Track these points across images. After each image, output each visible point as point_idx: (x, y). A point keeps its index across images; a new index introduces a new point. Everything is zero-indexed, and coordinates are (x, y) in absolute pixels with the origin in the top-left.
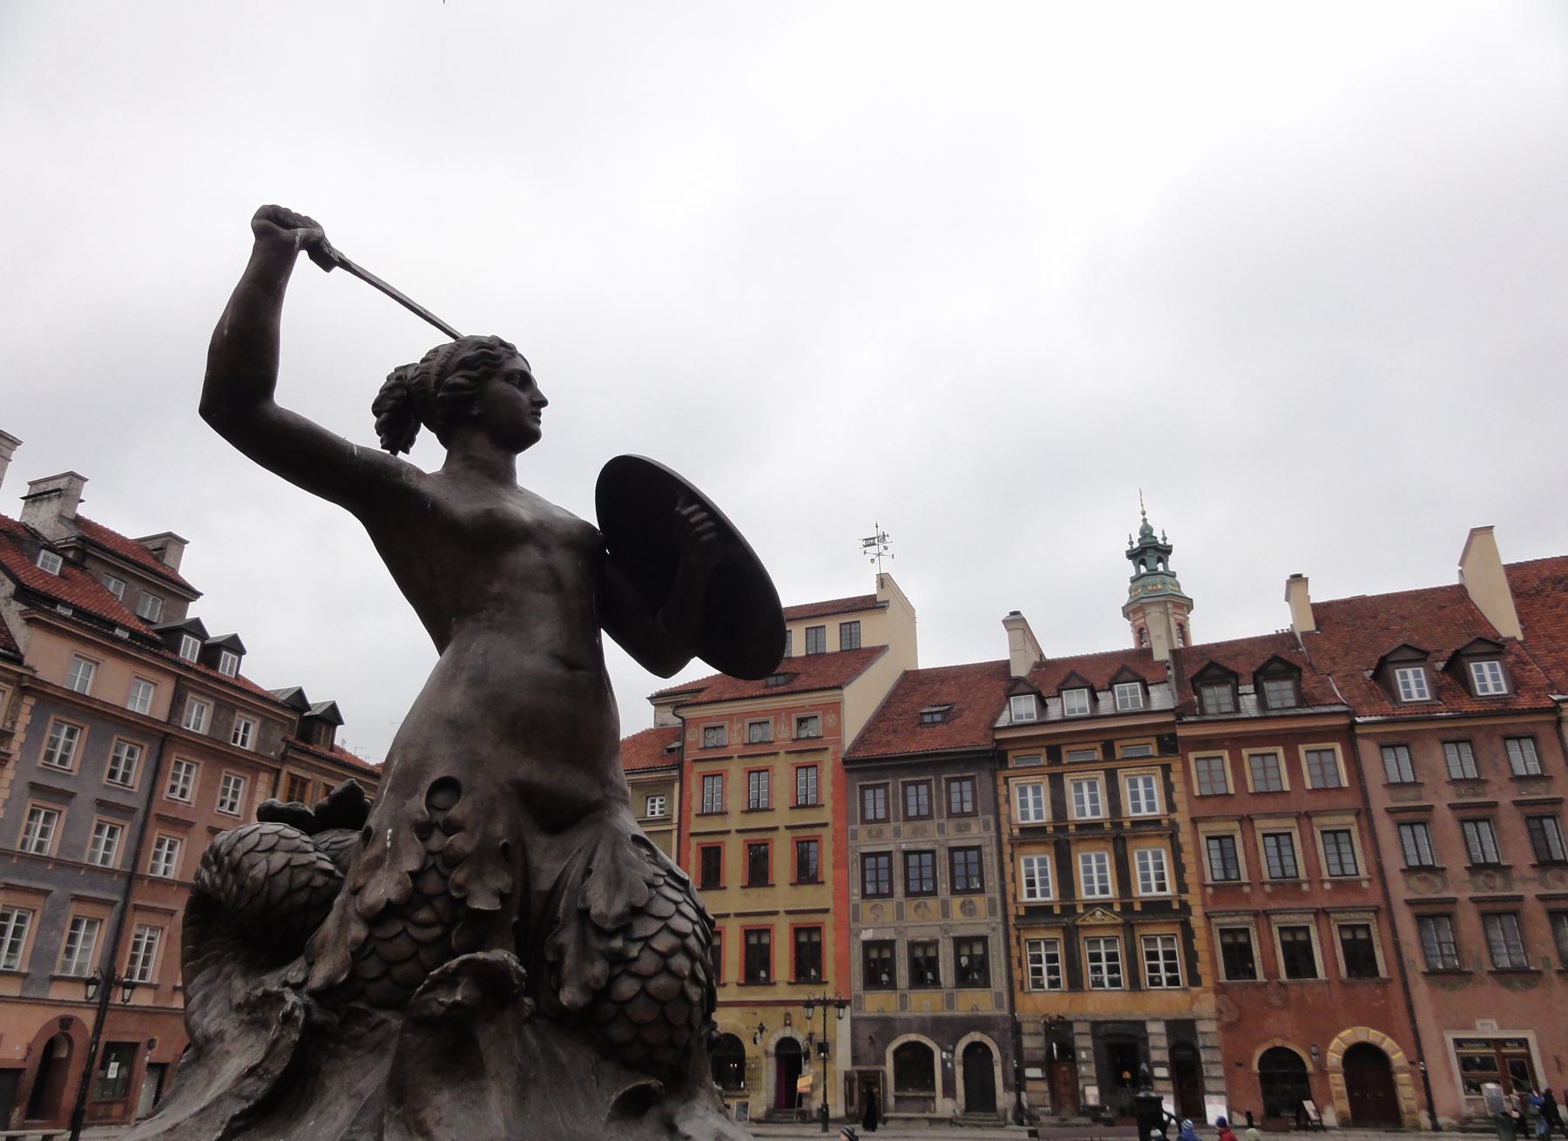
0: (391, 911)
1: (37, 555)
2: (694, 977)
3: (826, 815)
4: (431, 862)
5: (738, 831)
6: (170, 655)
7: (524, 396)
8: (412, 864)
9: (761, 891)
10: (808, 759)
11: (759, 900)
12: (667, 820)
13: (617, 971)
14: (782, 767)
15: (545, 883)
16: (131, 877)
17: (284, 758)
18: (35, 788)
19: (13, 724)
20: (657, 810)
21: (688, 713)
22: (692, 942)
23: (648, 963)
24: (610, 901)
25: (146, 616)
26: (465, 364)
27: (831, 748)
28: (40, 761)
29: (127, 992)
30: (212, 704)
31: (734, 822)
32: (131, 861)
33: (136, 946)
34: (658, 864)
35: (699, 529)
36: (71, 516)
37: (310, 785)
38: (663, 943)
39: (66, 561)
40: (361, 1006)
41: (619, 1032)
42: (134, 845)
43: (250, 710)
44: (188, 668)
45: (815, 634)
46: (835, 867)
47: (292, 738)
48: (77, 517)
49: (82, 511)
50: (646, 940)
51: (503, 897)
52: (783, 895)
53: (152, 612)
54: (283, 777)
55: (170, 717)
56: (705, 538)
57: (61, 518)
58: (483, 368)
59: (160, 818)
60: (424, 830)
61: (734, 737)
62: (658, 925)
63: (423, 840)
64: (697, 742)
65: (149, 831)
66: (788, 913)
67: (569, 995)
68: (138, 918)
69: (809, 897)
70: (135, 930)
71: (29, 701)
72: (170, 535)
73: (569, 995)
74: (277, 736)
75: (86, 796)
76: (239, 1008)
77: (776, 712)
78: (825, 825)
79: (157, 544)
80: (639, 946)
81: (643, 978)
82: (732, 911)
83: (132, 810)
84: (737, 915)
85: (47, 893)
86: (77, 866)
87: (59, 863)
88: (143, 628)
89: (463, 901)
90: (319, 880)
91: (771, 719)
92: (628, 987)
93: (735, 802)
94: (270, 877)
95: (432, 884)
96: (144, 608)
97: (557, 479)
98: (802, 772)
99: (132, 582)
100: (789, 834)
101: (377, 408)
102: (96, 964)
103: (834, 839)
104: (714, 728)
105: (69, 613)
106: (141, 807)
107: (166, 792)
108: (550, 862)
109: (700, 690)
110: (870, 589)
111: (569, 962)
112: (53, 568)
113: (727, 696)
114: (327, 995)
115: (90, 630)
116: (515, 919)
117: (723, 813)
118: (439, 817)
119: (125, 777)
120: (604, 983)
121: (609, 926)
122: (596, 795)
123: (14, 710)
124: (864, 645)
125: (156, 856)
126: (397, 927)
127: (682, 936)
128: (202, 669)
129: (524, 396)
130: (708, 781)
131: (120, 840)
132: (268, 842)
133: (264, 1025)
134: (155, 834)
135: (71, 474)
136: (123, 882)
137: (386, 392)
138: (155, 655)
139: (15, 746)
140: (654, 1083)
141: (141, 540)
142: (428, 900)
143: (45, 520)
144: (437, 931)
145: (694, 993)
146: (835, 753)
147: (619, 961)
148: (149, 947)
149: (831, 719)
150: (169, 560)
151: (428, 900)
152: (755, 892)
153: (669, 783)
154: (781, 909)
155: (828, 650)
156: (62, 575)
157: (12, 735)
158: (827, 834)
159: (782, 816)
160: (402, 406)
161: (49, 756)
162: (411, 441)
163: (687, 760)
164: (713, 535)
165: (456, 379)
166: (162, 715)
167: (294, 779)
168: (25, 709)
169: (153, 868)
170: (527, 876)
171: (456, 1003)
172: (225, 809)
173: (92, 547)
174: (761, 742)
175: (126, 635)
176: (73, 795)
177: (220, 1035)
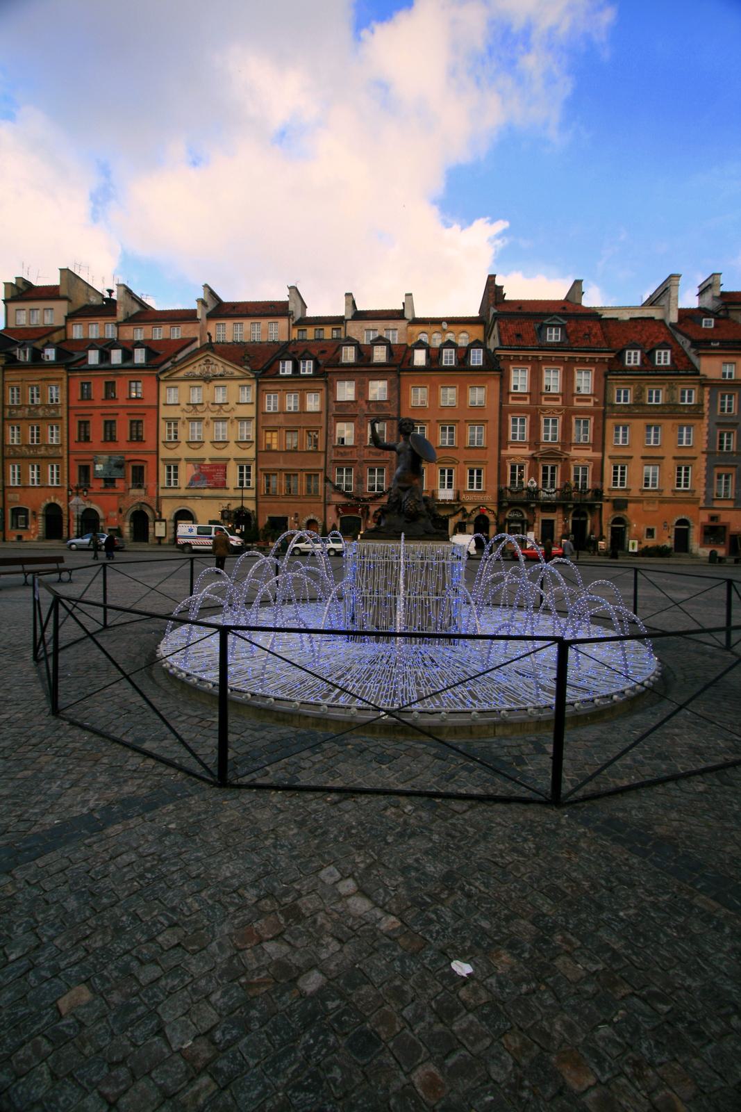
18: (718, 424)
19: (702, 400)
28: (719, 413)
36: (718, 294)
39: (718, 319)
49: (722, 289)
57: (714, 298)
71: (707, 389)
135: (713, 275)
139: (705, 409)
143: (708, 302)
156: (716, 326)
157: (702, 405)
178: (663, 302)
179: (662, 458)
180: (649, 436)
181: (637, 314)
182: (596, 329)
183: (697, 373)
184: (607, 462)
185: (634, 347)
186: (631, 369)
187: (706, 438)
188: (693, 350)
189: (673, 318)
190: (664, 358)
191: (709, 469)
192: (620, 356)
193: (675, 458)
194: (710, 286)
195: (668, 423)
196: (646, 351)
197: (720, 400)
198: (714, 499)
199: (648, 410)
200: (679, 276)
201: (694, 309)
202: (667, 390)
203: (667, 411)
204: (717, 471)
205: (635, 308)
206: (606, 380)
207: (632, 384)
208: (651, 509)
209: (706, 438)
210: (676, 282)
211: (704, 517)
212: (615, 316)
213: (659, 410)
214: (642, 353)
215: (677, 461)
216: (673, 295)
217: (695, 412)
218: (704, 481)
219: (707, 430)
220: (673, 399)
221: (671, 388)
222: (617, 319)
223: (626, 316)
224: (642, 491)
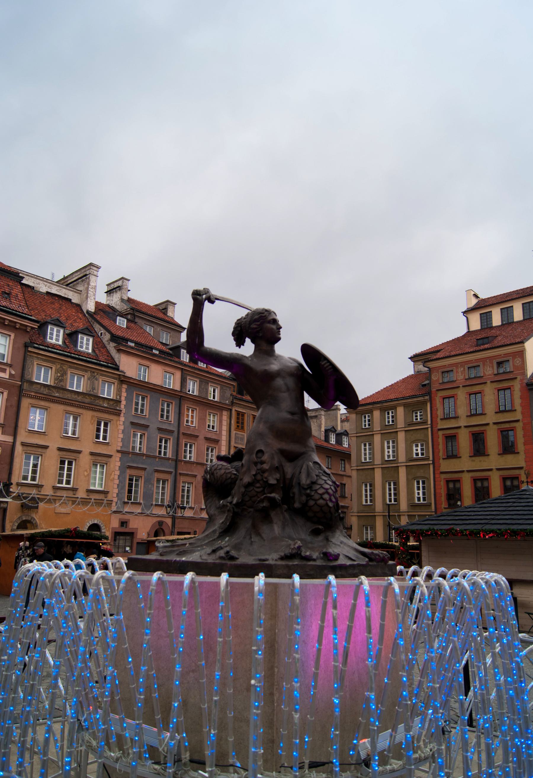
0: (249, 485)
1: (116, 319)
2: (331, 500)
3: (518, 416)
4: (258, 472)
5: (466, 427)
6: (177, 360)
7: (274, 327)
8: (254, 473)
9: (481, 458)
10: (505, 385)
12: (425, 423)
13: (309, 498)
14: (489, 392)
15: (289, 476)
16: (177, 461)
17: (232, 404)
18: (132, 423)
19: (120, 397)
20: (419, 417)
21: (432, 365)
22: (330, 491)
23: (317, 497)
24: (306, 480)
25: (164, 342)
26: (256, 321)
27: (519, 378)
29: (183, 510)
30: (198, 381)
31: (462, 422)
32: (175, 454)
33: (183, 491)
34: (321, 470)
35: (327, 369)
36: (126, 298)
37: (246, 416)
38: (321, 491)
39: (128, 320)
40: (245, 507)
41: (310, 514)
42: (175, 447)
43: (214, 382)
44: (185, 365)
45: (507, 313)
46: (525, 444)
47: (235, 394)
48: (128, 298)
49: (132, 295)
50: (316, 490)
51: (277, 480)
52: (494, 460)
53: (166, 339)
54: (234, 412)
55: (181, 389)
56: (330, 371)
57: (122, 300)
58: (261, 321)
59: (184, 434)
61: (460, 376)
62: (319, 486)
63: (256, 466)
64: (438, 380)
65: (180, 441)
66: (498, 469)
67: (297, 505)
68: (182, 479)
69: (510, 461)
70: (182, 484)
71: (125, 386)
72: (168, 301)
73: (297, 505)
74: (228, 393)
75: (153, 427)
76: (218, 508)
77: (484, 360)
78: (518, 421)
79: (163, 306)
80: (314, 492)
81: (316, 500)
82: (465, 469)
83: (172, 432)
84: (468, 471)
85: (145, 469)
86: (155, 457)
87: (148, 456)
88: (164, 348)
89: (267, 482)
90: (233, 476)
91: (481, 364)
92: (311, 503)
93: (462, 411)
94: (221, 476)
95: (259, 477)
96: (163, 338)
97: (288, 350)
98: (502, 392)
99: (156, 326)
100: (496, 427)
101: (233, 334)
102: (168, 499)
103: (524, 429)
104: (448, 372)
105: (133, 345)
106: (175, 429)
107: (185, 423)
108: (289, 469)
109: (438, 351)
111: (297, 497)
112: (123, 325)
113: (452, 353)
114: (237, 505)
115: (143, 352)
116: (282, 485)
117: (456, 418)
118: (259, 460)
119: (168, 417)
120: (305, 501)
121: (306, 487)
122: (303, 450)
123: (119, 392)
125: (185, 451)
126: (252, 488)
127: (327, 489)
128: (192, 365)
129: (274, 327)
130: (446, 401)
131: (170, 445)
132: (220, 467)
133: (224, 512)
134: (183, 441)
135: (122, 278)
136: (174, 463)
137: (235, 328)
138: (171, 360)
139: (122, 407)
140: (320, 527)
141: (156, 306)
142: (258, 481)
144: (261, 489)
145: (331, 504)
146: (521, 380)
147: (309, 496)
148: (188, 491)
149: (518, 361)
150: (170, 314)
151: (258, 481)
152: (477, 459)
153: (424, 403)
154: (494, 468)
156: (128, 327)
157: (120, 402)
158: (519, 426)
159: (491, 418)
160: (240, 333)
161: (136, 410)
162: (244, 341)
163: (434, 390)
164: (332, 370)
165: (253, 326)
166: (178, 388)
167: (238, 413)
168: (124, 390)
169: (185, 457)
170: (284, 474)
171: (264, 507)
172: (211, 429)
173: (136, 311)
174: (475, 377)
175: (157, 352)
176: (147, 426)
177: (215, 514)
178: (80, 287)
179: (79, 452)
180: (67, 425)
181: (54, 290)
182: (17, 290)
183: (118, 369)
184: (19, 448)
185: (58, 323)
186: (53, 346)
187: (121, 436)
188: (112, 345)
189: (91, 307)
190: (86, 345)
191: (123, 469)
192: (43, 326)
193: (92, 454)
194: (119, 287)
195: (88, 415)
196: (68, 332)
197: (134, 400)
198: (125, 503)
199: (69, 396)
200: (98, 268)
201: (103, 304)
202: (89, 379)
203: (87, 400)
204: (129, 472)
205: (51, 282)
206: (26, 351)
207: (53, 363)
208: (63, 510)
209: (121, 436)
210: (95, 273)
211: (115, 523)
212: (31, 284)
213: (79, 398)
214: (64, 332)
215: (93, 458)
216: (92, 284)
217: (112, 408)
218: (117, 482)
219: (122, 427)
220: (94, 389)
221: (92, 378)
222: (33, 287)
223: (43, 288)
224: (55, 488)
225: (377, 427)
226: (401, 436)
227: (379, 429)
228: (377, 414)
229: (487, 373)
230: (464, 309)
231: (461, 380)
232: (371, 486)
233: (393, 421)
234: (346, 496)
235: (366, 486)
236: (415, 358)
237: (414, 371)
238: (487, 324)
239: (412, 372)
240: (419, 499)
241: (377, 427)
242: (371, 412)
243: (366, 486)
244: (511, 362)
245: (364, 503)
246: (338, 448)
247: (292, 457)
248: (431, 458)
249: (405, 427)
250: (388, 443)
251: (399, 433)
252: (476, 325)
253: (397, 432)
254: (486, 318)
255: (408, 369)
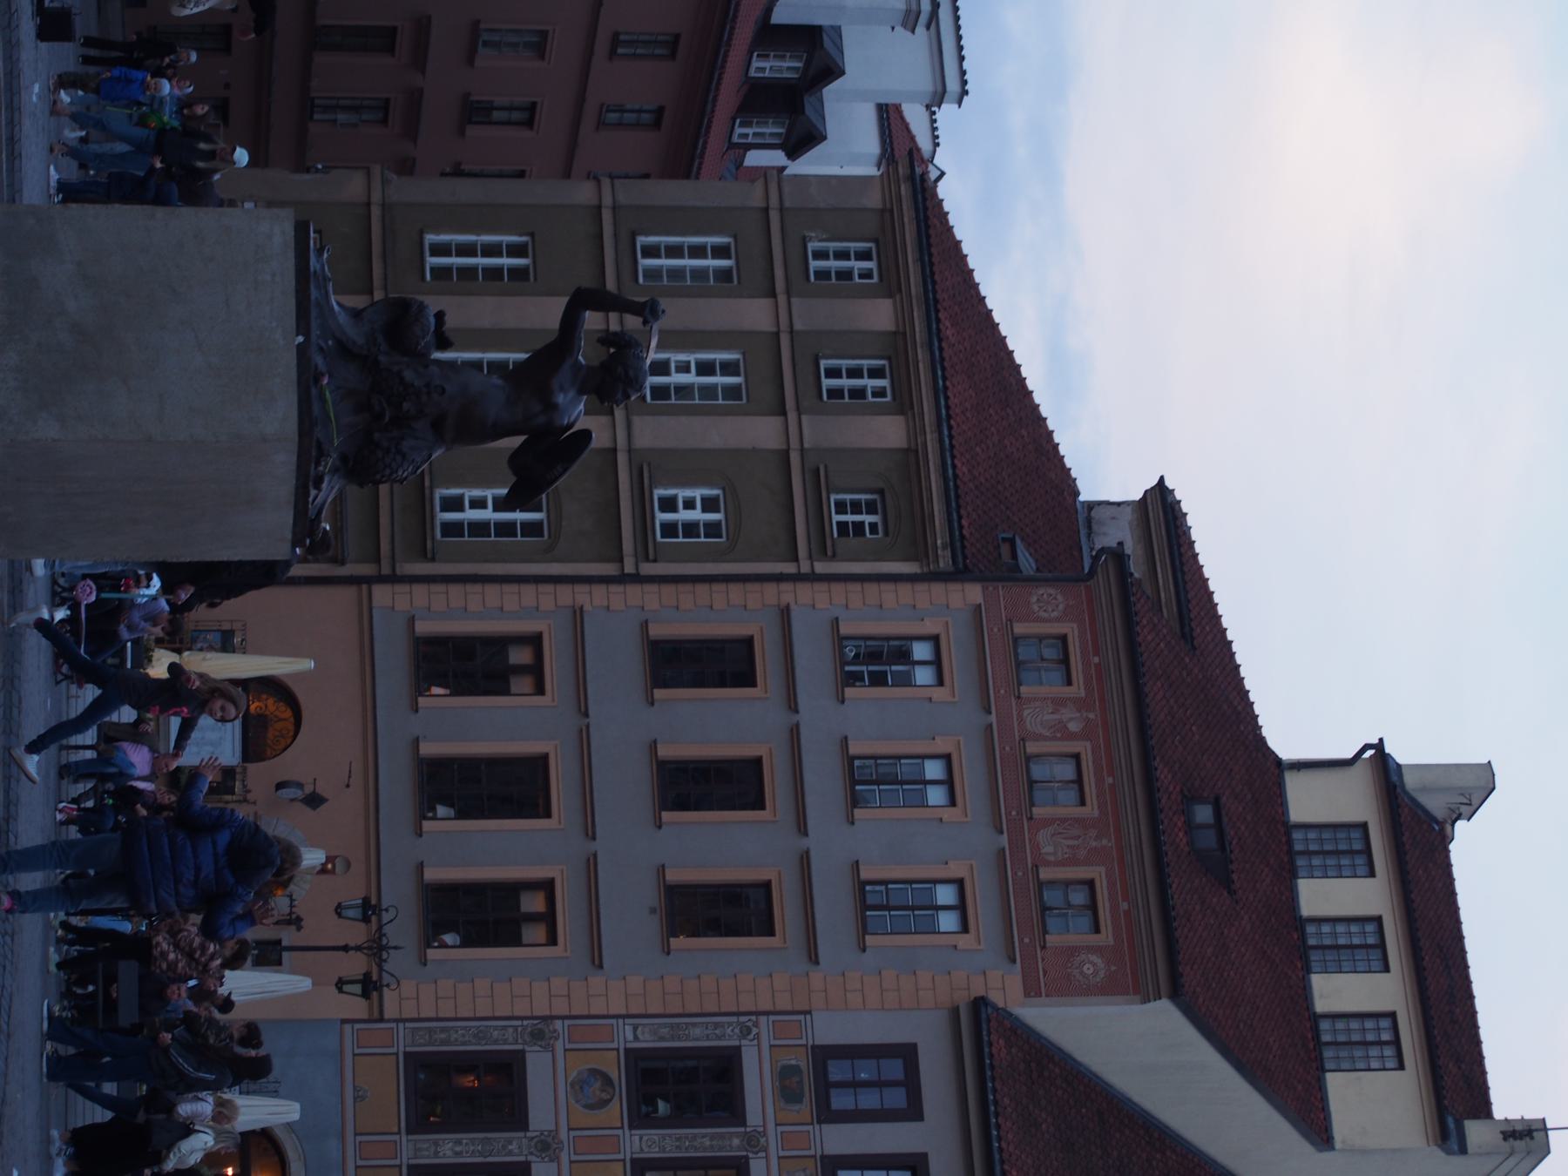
11: (625, 787)
12: (823, 550)
45: (1359, 946)
60: (427, 385)
69: (631, 913)
73: (376, 436)
110: (1507, 1103)
124: (1335, 1082)
153: (919, 548)
155: (1318, 981)
225: (811, 314)
226: (762, 432)
227: (798, 326)
228: (879, 315)
229: (1043, 836)
230: (1402, 753)
231: (1021, 720)
232: (518, 274)
233: (836, 393)
234: (472, 131)
235: (516, 250)
236: (1161, 510)
237: (1091, 506)
238: (1308, 853)
239: (1088, 491)
240: (455, 504)
241: (811, 314)
242: (890, 285)
243: (516, 250)
244: (1093, 939)
245: (430, 238)
246: (728, 95)
247: (437, 426)
248: (647, 569)
249: (802, 449)
250: (728, 368)
251: (775, 422)
252: (1306, 803)
253: (784, 413)
254: (1343, 848)
255: (1106, 471)
